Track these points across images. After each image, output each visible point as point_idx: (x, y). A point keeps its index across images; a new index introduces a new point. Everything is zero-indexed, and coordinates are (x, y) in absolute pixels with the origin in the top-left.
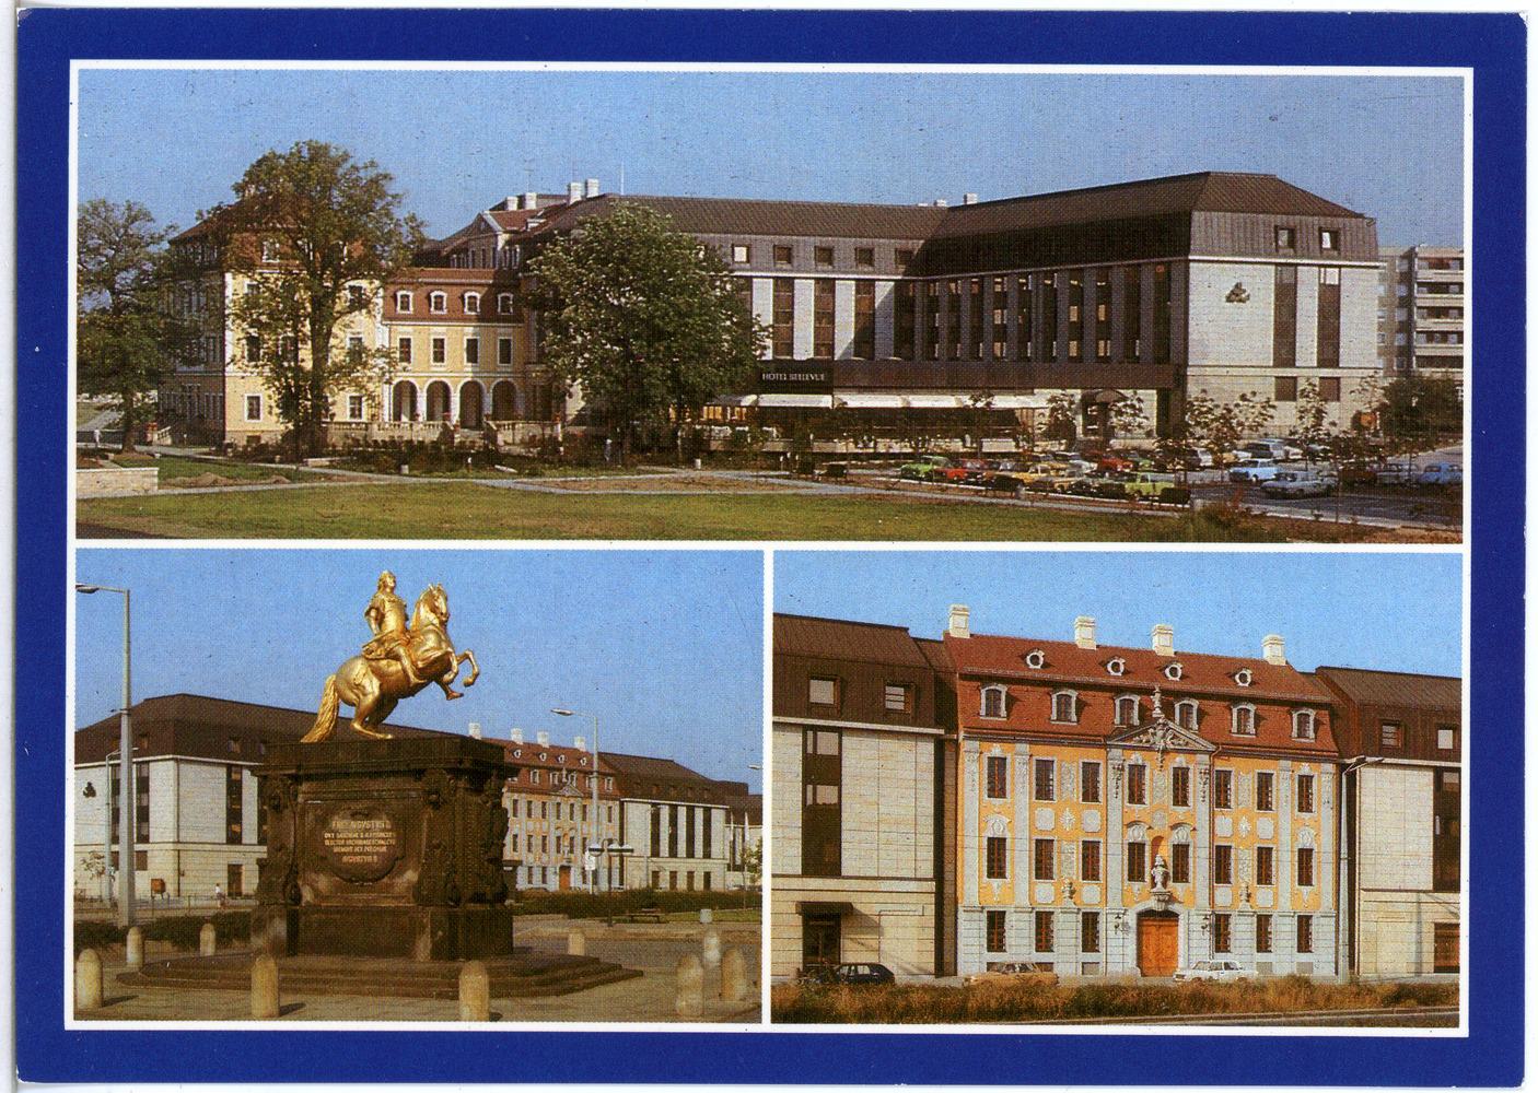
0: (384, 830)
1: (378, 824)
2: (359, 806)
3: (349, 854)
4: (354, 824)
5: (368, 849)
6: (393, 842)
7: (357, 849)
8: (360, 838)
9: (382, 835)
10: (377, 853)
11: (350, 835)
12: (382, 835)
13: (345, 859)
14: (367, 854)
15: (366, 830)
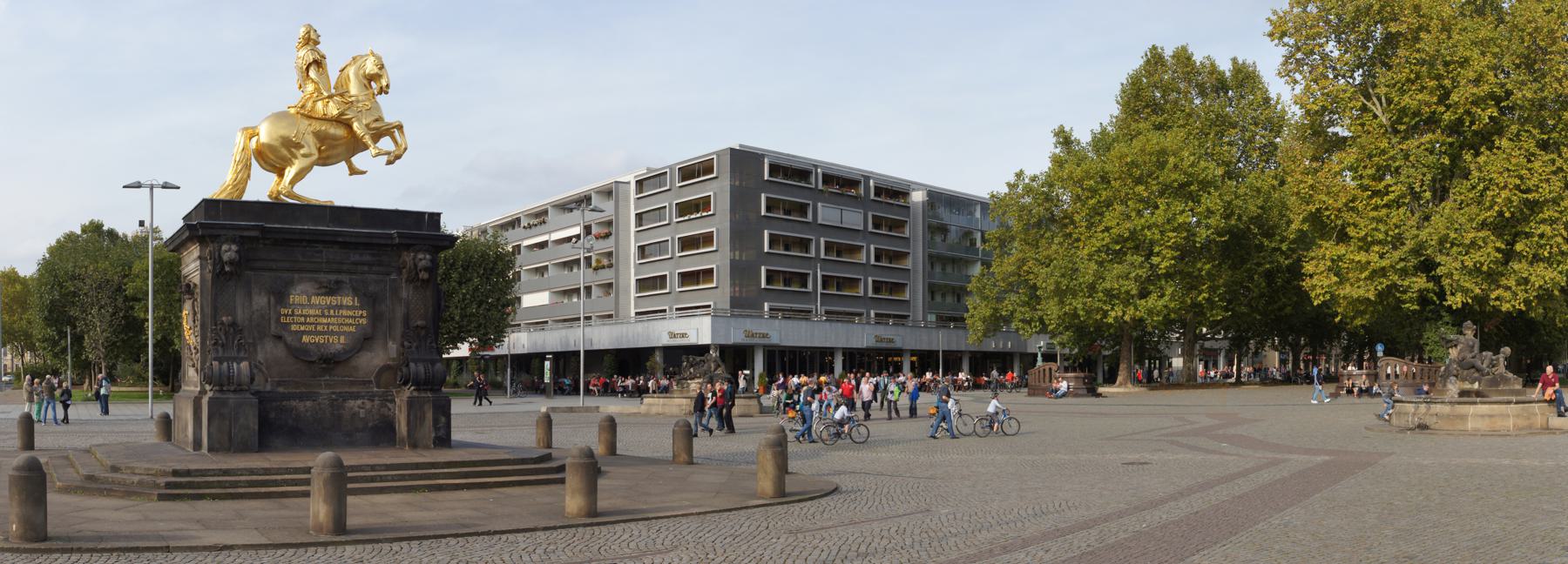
0: (348, 308)
1: (347, 301)
2: (323, 277)
3: (309, 333)
4: (315, 300)
5: (336, 329)
6: (364, 321)
7: (319, 328)
8: (323, 316)
9: (350, 313)
10: (344, 333)
11: (312, 312)
12: (350, 313)
13: (305, 339)
14: (332, 333)
15: (329, 308)
